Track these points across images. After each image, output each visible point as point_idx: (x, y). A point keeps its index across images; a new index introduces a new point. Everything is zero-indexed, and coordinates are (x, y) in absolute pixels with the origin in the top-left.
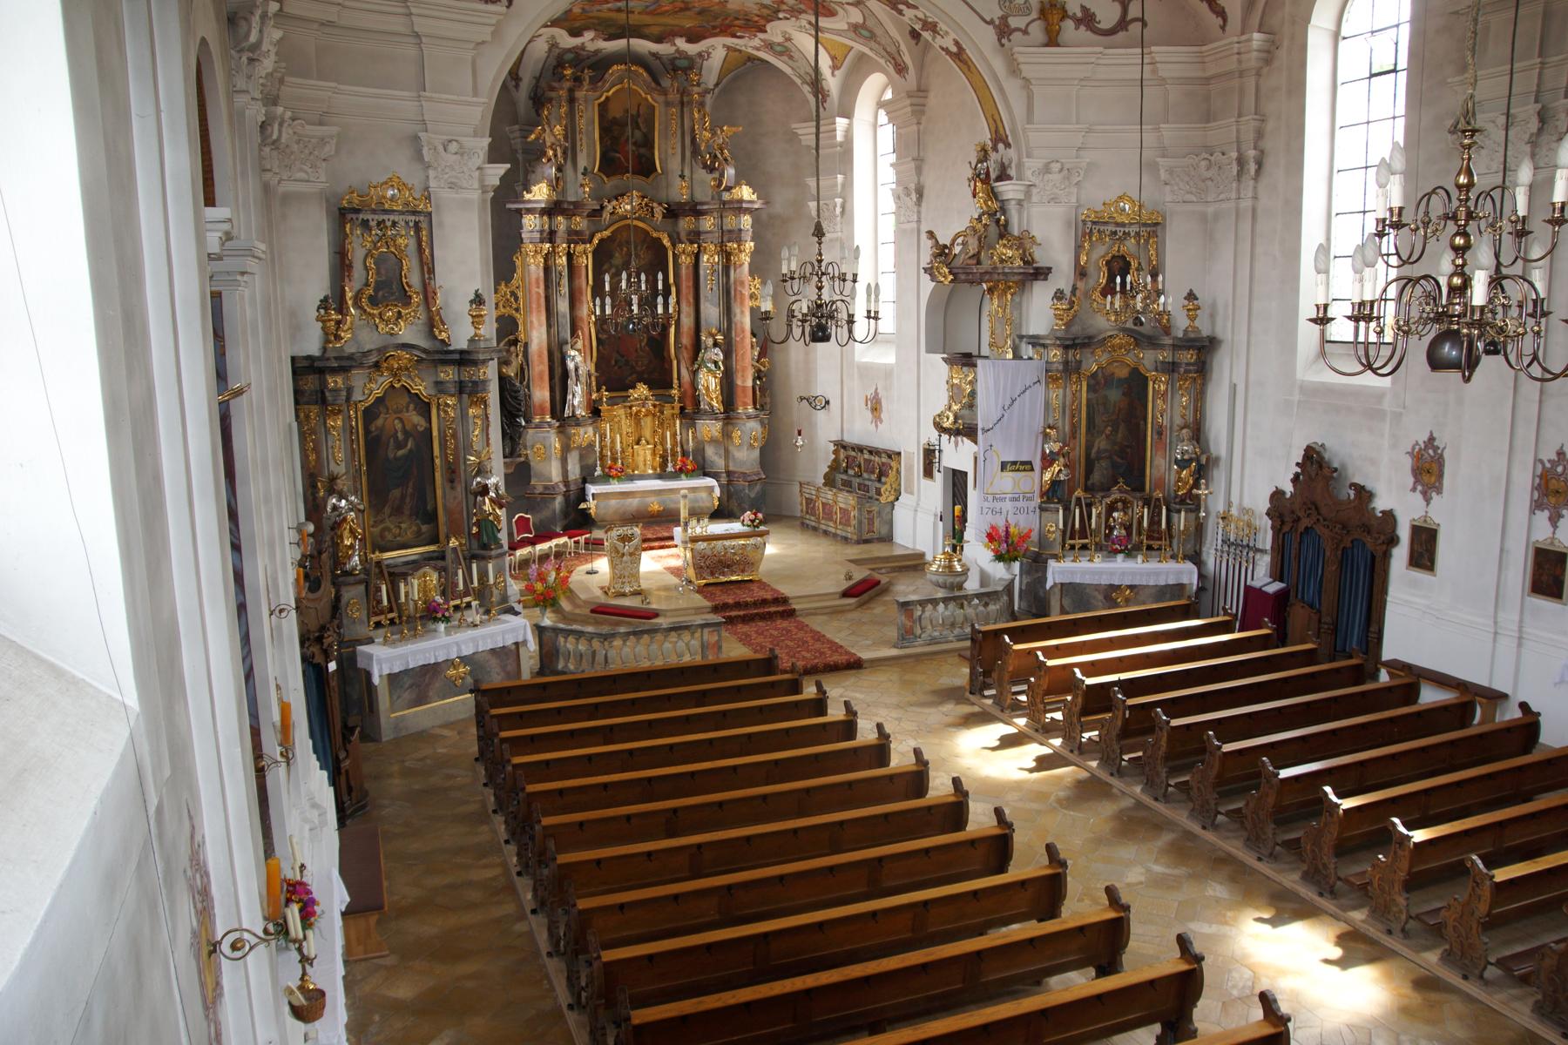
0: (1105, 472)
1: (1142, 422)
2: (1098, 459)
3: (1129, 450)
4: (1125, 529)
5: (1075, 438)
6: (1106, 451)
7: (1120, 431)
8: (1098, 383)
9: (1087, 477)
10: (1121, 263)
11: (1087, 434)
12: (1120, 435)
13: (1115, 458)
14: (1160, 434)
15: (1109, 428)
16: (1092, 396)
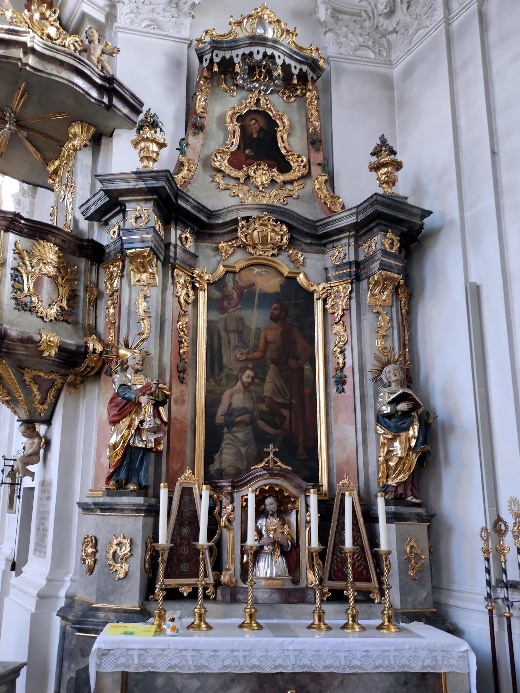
0: (243, 450)
1: (307, 367)
2: (230, 424)
3: (285, 412)
4: (283, 554)
5: (182, 381)
6: (244, 411)
7: (268, 378)
8: (226, 297)
9: (209, 460)
10: (262, 122)
11: (207, 379)
12: (268, 388)
13: (262, 424)
14: (341, 382)
15: (248, 372)
16: (216, 316)
